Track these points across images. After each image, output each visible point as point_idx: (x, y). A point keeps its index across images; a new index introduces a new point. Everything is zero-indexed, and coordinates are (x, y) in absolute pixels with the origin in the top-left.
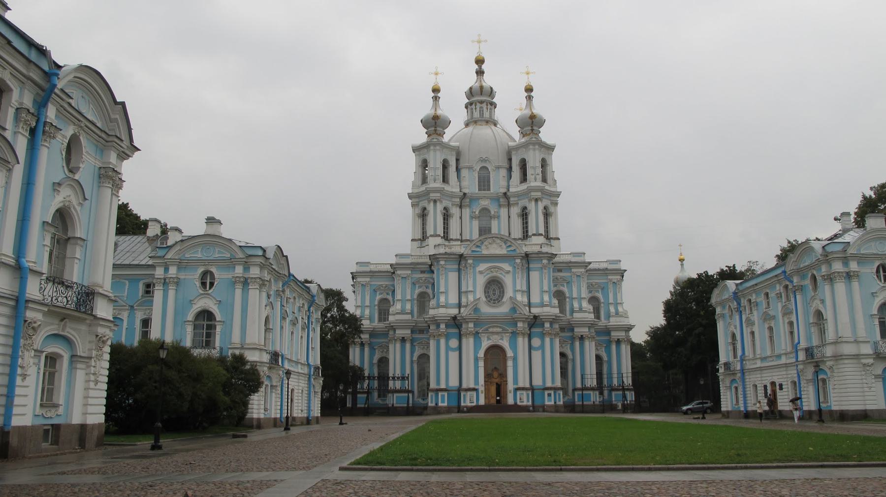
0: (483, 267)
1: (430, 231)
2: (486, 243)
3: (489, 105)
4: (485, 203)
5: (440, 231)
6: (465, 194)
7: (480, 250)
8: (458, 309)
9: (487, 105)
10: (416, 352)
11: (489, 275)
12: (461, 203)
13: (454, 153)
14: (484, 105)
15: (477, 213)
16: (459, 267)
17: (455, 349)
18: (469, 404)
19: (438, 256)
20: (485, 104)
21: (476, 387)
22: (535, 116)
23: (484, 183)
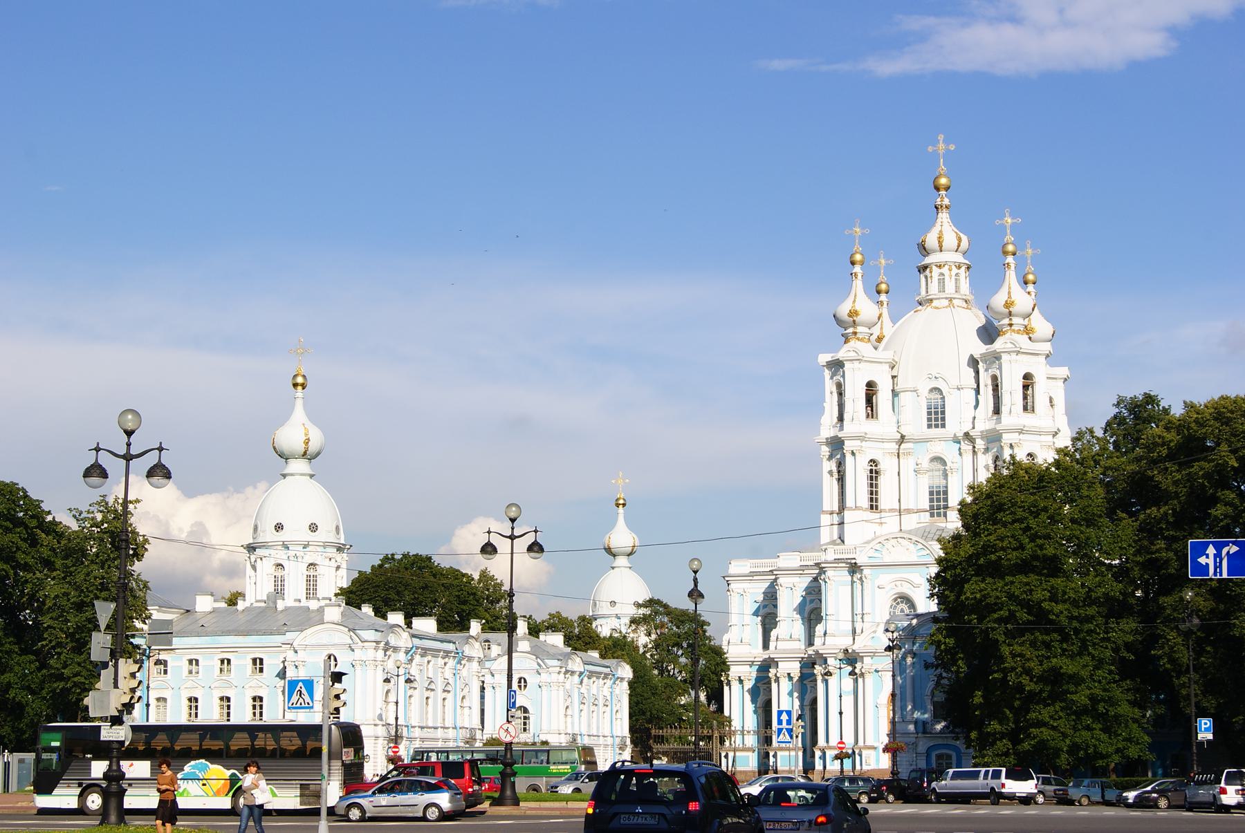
0: (885, 578)
1: (849, 502)
2: (888, 545)
3: (954, 267)
4: (939, 449)
5: (864, 501)
6: (903, 437)
7: (880, 556)
8: (852, 638)
9: (950, 270)
10: (809, 691)
11: (894, 590)
12: (899, 449)
13: (886, 367)
14: (945, 270)
15: (925, 464)
16: (852, 579)
17: (849, 692)
18: (865, 768)
19: (823, 565)
20: (947, 267)
21: (875, 745)
22: (1013, 302)
23: (937, 417)
